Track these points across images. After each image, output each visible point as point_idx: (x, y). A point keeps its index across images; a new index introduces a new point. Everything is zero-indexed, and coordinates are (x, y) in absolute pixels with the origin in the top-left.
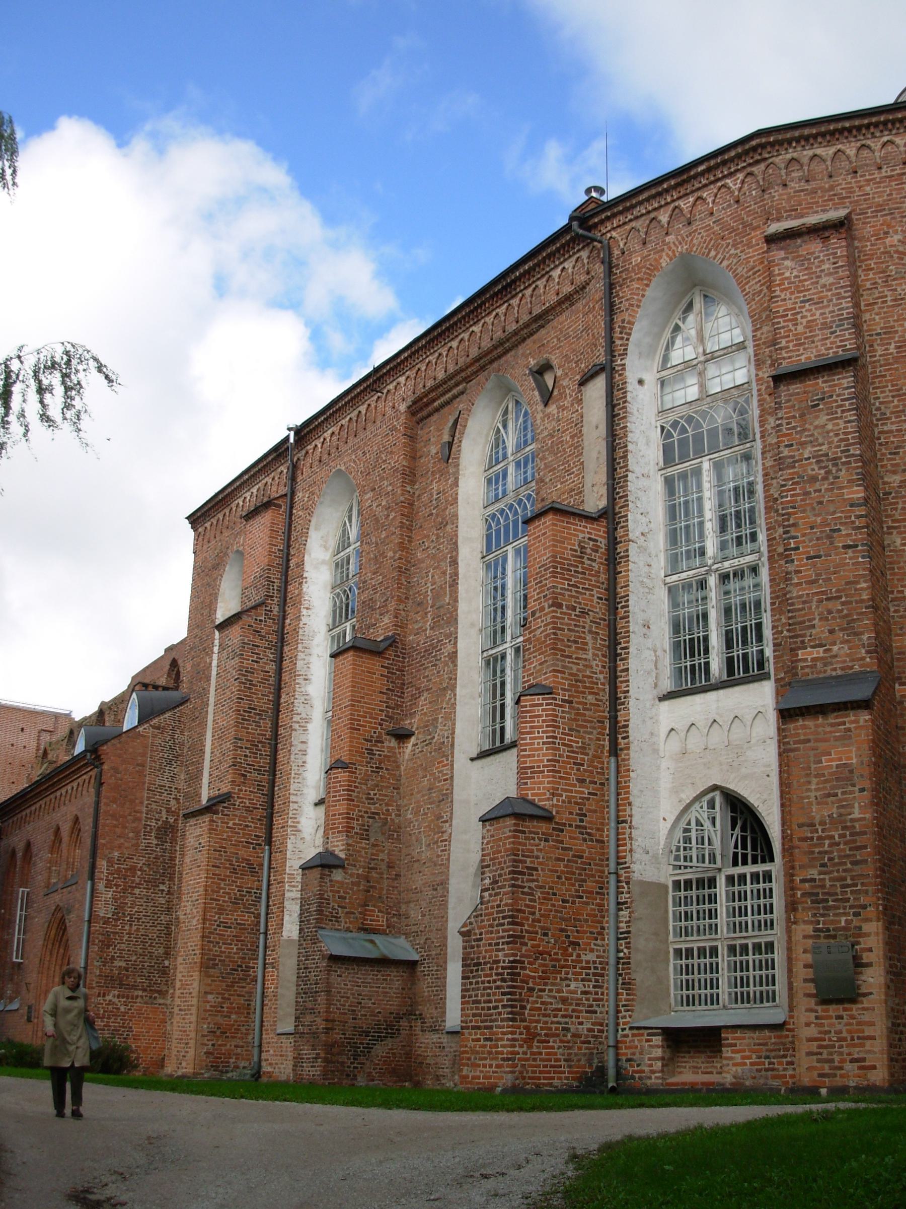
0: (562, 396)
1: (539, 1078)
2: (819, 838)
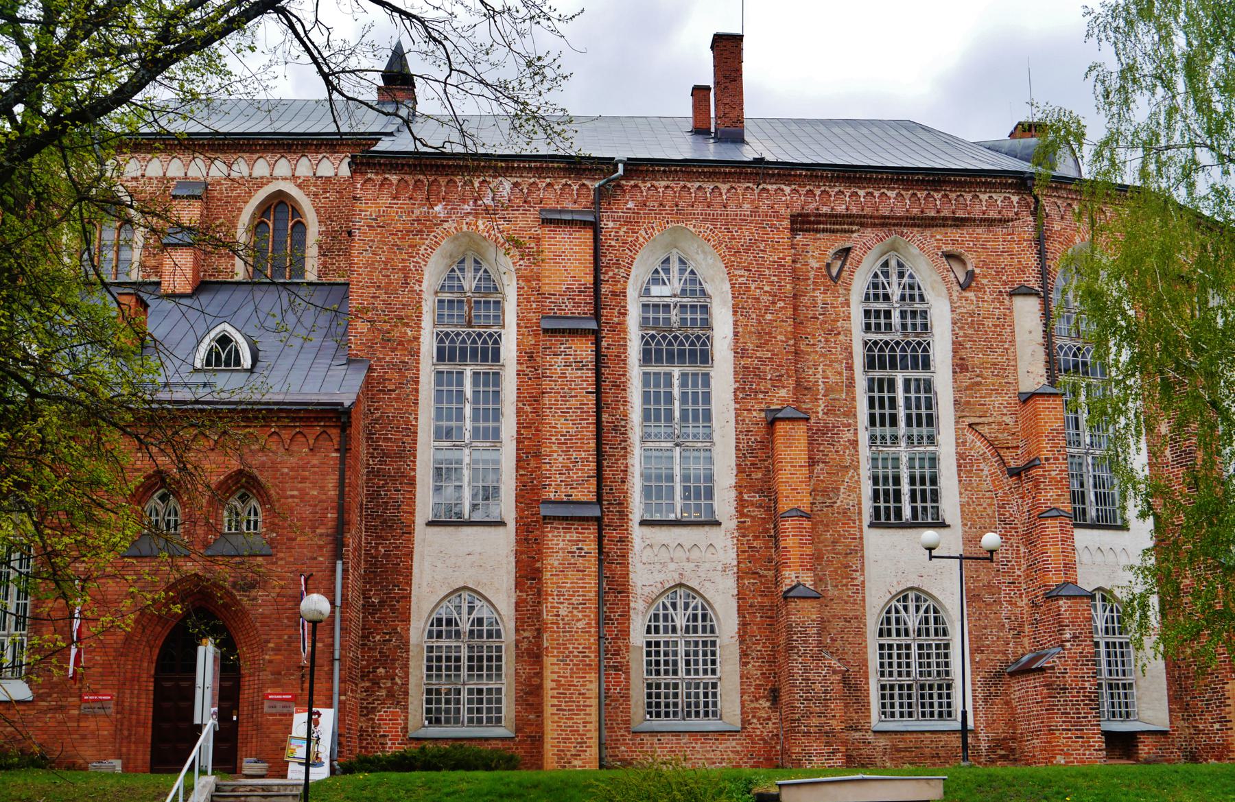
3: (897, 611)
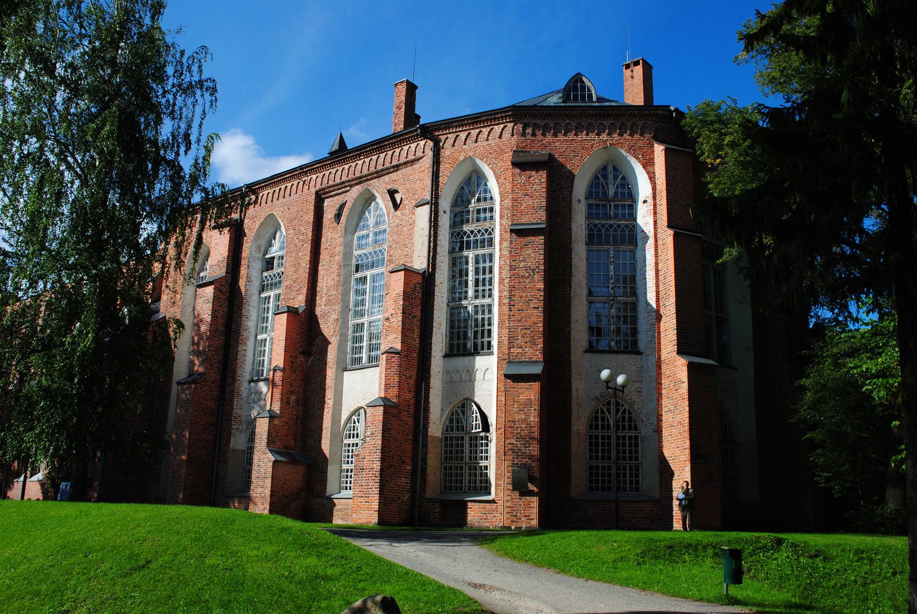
0: (404, 208)
1: (388, 519)
2: (517, 427)
3: (603, 412)
